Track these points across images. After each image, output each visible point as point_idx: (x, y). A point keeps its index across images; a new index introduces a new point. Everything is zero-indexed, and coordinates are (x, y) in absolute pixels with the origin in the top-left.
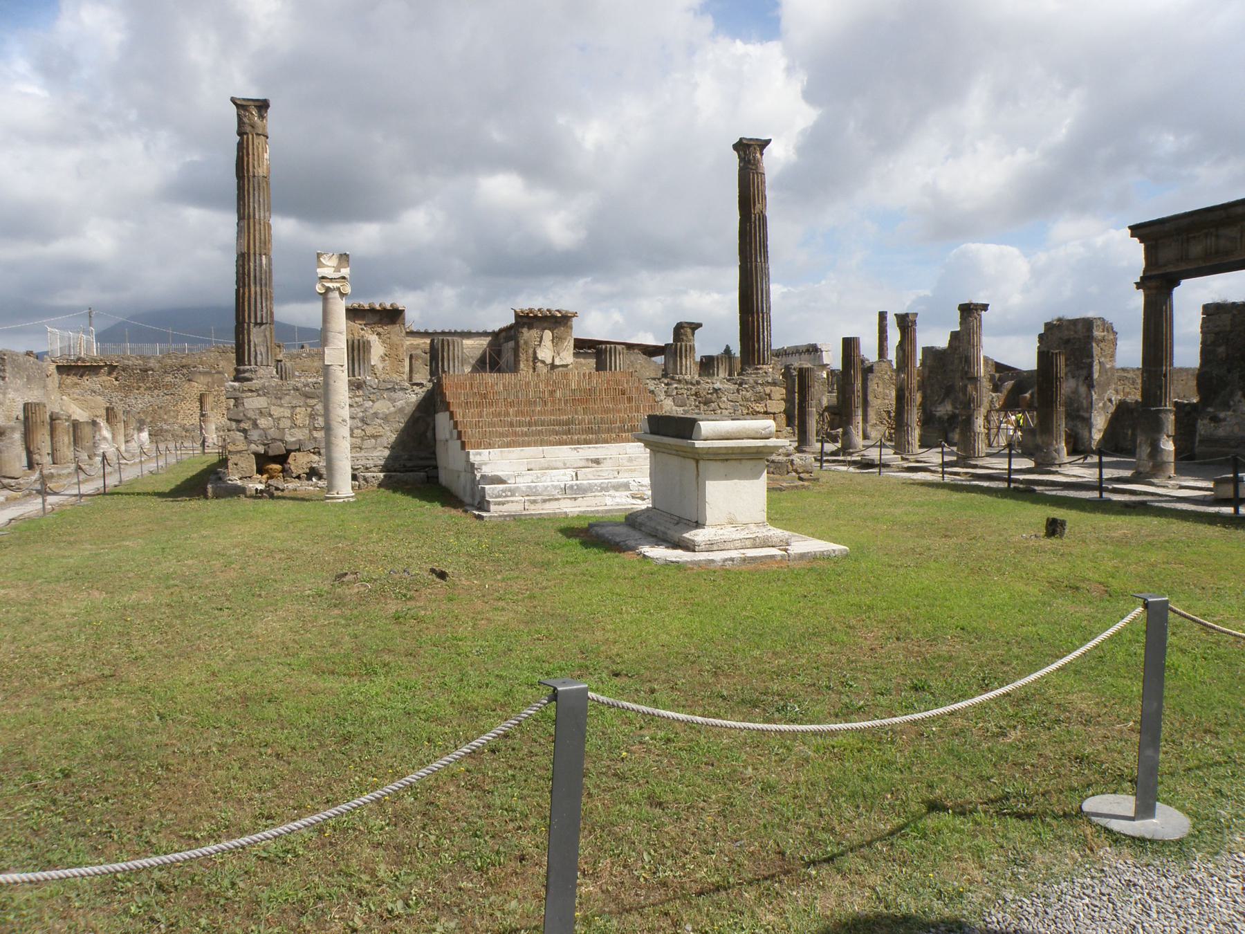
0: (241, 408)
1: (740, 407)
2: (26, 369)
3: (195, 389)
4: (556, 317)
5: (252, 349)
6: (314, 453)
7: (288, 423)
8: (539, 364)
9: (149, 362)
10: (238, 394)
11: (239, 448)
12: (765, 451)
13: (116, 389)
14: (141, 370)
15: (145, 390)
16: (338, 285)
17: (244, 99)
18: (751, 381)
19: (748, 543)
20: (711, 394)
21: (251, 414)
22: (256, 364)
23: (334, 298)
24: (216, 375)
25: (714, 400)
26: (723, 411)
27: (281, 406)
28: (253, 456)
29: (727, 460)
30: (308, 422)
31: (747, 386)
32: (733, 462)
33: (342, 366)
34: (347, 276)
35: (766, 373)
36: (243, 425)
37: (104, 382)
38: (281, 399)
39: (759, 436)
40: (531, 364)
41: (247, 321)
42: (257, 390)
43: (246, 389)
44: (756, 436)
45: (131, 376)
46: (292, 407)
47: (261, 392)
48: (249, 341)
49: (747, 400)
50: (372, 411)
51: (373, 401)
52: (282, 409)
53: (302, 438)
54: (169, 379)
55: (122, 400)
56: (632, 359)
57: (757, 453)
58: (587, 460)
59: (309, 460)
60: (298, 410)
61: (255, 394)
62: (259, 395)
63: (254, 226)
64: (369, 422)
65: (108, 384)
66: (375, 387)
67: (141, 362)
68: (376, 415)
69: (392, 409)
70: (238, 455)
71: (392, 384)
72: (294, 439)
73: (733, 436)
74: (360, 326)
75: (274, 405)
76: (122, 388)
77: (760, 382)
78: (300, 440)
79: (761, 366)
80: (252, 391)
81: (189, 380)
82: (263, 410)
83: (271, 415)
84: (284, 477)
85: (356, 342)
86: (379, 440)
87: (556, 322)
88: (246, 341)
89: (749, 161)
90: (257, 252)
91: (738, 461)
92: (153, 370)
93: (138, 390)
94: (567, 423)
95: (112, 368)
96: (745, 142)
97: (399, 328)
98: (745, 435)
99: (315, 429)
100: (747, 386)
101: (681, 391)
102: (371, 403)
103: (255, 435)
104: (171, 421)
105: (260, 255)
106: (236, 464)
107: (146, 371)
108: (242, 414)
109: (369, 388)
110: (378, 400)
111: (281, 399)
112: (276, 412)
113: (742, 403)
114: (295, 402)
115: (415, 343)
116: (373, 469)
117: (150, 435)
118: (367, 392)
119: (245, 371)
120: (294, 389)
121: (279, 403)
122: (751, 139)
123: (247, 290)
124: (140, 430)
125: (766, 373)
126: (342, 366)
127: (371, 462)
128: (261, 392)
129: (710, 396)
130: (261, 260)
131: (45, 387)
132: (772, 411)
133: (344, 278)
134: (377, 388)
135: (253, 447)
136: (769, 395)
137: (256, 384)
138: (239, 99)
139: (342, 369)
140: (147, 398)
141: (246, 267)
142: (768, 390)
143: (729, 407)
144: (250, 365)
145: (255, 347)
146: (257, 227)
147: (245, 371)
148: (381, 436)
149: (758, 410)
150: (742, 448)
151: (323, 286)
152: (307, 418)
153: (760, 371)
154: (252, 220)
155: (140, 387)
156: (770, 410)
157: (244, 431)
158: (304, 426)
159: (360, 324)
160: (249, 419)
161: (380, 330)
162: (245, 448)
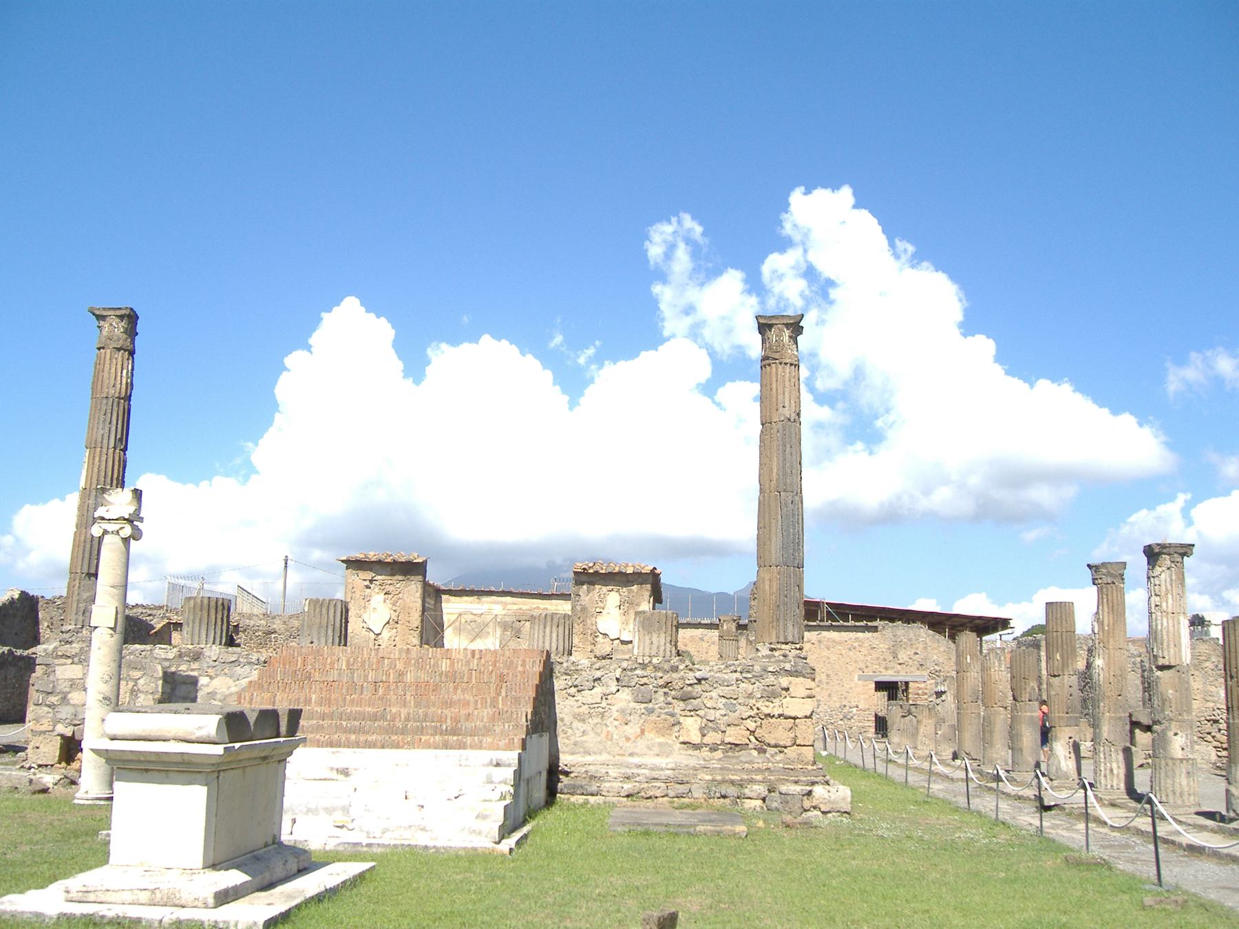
0: (51, 678)
1: (738, 706)
4: (626, 574)
8: (600, 639)
10: (50, 660)
11: (43, 728)
12: (194, 760)
17: (104, 309)
18: (757, 668)
19: (144, 897)
20: (691, 685)
21: (63, 687)
25: (694, 694)
26: (712, 711)
29: (147, 770)
30: (128, 699)
31: (749, 675)
32: (157, 773)
35: (785, 656)
36: (53, 699)
39: (193, 737)
40: (590, 638)
42: (74, 656)
44: (188, 737)
45: (251, 639)
49: (750, 696)
50: (210, 690)
51: (211, 678)
56: (912, 635)
57: (183, 763)
58: (332, 769)
61: (70, 661)
69: (234, 689)
71: (236, 655)
73: (153, 734)
77: (770, 669)
79: (779, 646)
85: (206, 602)
87: (628, 581)
89: (770, 348)
91: (163, 774)
94: (375, 718)
96: (762, 321)
97: (414, 586)
98: (170, 735)
100: (749, 675)
101: (645, 680)
102: (208, 678)
106: (38, 748)
108: (51, 686)
109: (207, 659)
110: (217, 675)
113: (740, 701)
115: (525, 607)
118: (205, 665)
122: (773, 317)
125: (785, 656)
128: (76, 660)
129: (690, 688)
132: (793, 715)
135: (60, 728)
136: (787, 689)
138: (99, 309)
142: (784, 681)
143: (721, 706)
149: (767, 711)
150: (157, 754)
152: (128, 694)
153: (776, 654)
156: (788, 713)
161: (391, 588)
162: (51, 728)
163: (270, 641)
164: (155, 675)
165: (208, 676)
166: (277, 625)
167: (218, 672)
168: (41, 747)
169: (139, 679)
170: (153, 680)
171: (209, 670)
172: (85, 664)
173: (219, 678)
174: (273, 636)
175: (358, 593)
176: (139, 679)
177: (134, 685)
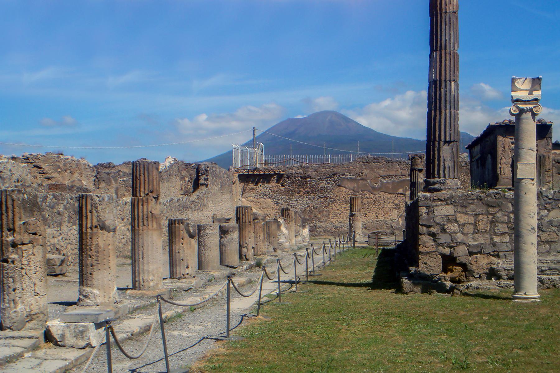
2: (221, 178)
3: (343, 193)
5: (442, 164)
6: (493, 256)
7: (471, 229)
9: (308, 171)
11: (428, 250)
13: (281, 193)
14: (301, 178)
15: (304, 194)
16: (531, 106)
22: (445, 177)
23: (527, 118)
24: (360, 182)
27: (466, 213)
28: (440, 257)
30: (489, 228)
33: (533, 180)
34: (540, 98)
37: (273, 187)
38: (466, 207)
41: (437, 139)
43: (436, 198)
45: (293, 182)
46: (476, 215)
47: (448, 202)
48: (439, 157)
50: (547, 219)
51: (549, 211)
52: (466, 217)
53: (483, 242)
54: (323, 184)
55: (286, 202)
59: (489, 261)
60: (481, 217)
62: (447, 204)
63: (446, 56)
64: (544, 229)
65: (276, 189)
66: (551, 197)
67: (301, 171)
68: (551, 223)
70: (428, 256)
72: (476, 243)
74: (511, 141)
75: (460, 213)
76: (286, 192)
78: (482, 244)
80: (441, 200)
81: (339, 186)
82: (450, 217)
83: (456, 221)
84: (466, 276)
86: (553, 245)
88: (436, 157)
90: (448, 79)
92: (310, 177)
93: (299, 193)
95: (280, 177)
99: (495, 234)
102: (546, 212)
103: (444, 238)
104: (324, 219)
105: (450, 81)
107: (305, 178)
109: (545, 198)
110: (553, 209)
111: (466, 207)
112: (462, 218)
114: (478, 210)
116: (548, 272)
117: (310, 231)
118: (543, 202)
119: (435, 183)
120: (477, 199)
121: (464, 211)
123: (438, 113)
124: (304, 227)
126: (533, 180)
127: (545, 265)
130: (451, 85)
131: (231, 192)
133: (536, 100)
134: (553, 199)
137: (444, 194)
139: (532, 182)
140: (306, 200)
141: (438, 93)
144: (439, 177)
145: (444, 162)
146: (448, 58)
147: (435, 183)
148: (555, 242)
151: (517, 107)
152: (488, 225)
154: (443, 52)
155: (301, 191)
157: (433, 235)
158: (485, 232)
159: (511, 139)
160: (438, 224)
162: (434, 250)
163: (307, 183)
164: (507, 210)
165: (546, 209)
166: (310, 172)
167: (554, 207)
168: (429, 263)
169: (496, 213)
170: (506, 214)
171: (547, 206)
172: (455, 205)
173: (555, 210)
174: (308, 179)
175: (507, 147)
176: (496, 213)
177: (493, 218)
